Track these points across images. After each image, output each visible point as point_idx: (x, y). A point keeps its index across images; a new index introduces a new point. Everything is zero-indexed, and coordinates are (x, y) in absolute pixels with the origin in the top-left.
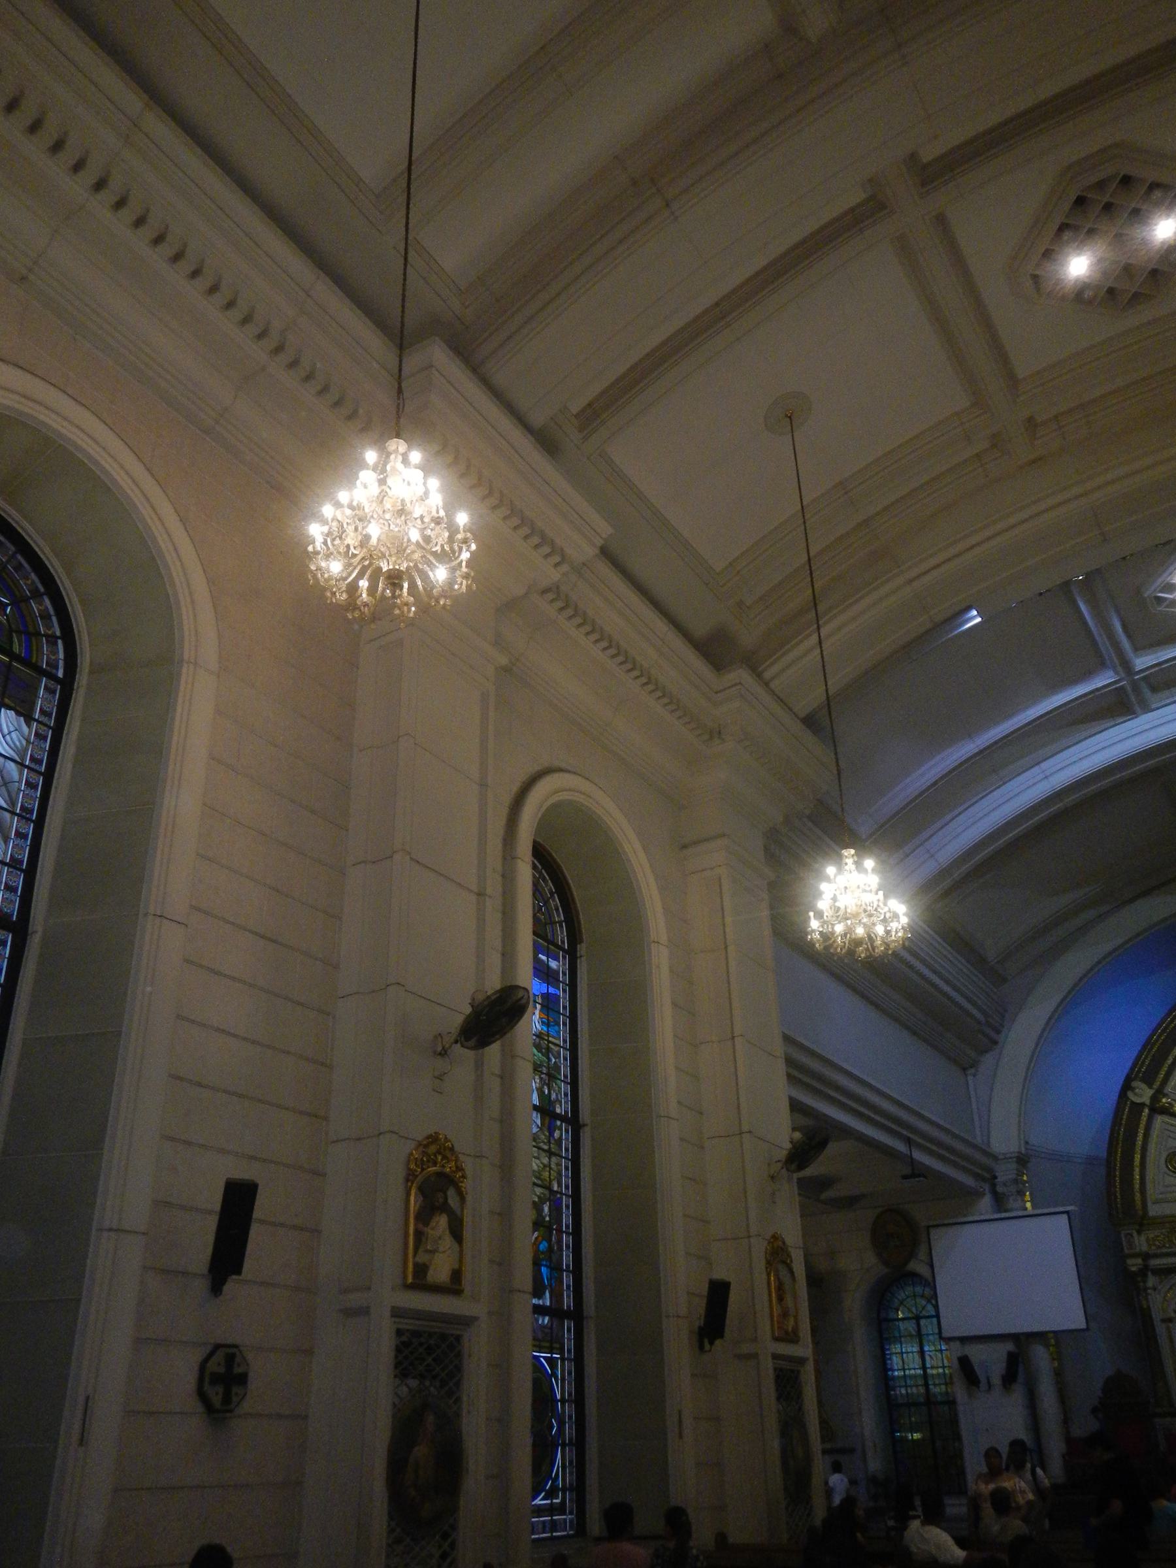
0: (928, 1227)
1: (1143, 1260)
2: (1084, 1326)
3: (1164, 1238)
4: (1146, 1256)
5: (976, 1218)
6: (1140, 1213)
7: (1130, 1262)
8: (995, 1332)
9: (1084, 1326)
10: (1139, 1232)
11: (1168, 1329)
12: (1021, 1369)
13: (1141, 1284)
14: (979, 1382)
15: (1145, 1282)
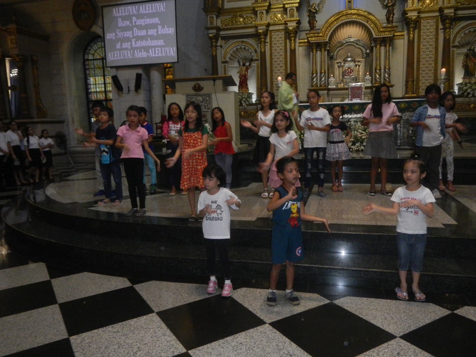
0: (103, 7)
1: (216, 31)
2: (176, 60)
3: (229, 21)
4: (219, 29)
6: (220, 6)
7: (210, 31)
8: (135, 64)
9: (176, 60)
10: (217, 17)
11: (225, 66)
12: (144, 83)
14: (123, 89)
15: (216, 42)
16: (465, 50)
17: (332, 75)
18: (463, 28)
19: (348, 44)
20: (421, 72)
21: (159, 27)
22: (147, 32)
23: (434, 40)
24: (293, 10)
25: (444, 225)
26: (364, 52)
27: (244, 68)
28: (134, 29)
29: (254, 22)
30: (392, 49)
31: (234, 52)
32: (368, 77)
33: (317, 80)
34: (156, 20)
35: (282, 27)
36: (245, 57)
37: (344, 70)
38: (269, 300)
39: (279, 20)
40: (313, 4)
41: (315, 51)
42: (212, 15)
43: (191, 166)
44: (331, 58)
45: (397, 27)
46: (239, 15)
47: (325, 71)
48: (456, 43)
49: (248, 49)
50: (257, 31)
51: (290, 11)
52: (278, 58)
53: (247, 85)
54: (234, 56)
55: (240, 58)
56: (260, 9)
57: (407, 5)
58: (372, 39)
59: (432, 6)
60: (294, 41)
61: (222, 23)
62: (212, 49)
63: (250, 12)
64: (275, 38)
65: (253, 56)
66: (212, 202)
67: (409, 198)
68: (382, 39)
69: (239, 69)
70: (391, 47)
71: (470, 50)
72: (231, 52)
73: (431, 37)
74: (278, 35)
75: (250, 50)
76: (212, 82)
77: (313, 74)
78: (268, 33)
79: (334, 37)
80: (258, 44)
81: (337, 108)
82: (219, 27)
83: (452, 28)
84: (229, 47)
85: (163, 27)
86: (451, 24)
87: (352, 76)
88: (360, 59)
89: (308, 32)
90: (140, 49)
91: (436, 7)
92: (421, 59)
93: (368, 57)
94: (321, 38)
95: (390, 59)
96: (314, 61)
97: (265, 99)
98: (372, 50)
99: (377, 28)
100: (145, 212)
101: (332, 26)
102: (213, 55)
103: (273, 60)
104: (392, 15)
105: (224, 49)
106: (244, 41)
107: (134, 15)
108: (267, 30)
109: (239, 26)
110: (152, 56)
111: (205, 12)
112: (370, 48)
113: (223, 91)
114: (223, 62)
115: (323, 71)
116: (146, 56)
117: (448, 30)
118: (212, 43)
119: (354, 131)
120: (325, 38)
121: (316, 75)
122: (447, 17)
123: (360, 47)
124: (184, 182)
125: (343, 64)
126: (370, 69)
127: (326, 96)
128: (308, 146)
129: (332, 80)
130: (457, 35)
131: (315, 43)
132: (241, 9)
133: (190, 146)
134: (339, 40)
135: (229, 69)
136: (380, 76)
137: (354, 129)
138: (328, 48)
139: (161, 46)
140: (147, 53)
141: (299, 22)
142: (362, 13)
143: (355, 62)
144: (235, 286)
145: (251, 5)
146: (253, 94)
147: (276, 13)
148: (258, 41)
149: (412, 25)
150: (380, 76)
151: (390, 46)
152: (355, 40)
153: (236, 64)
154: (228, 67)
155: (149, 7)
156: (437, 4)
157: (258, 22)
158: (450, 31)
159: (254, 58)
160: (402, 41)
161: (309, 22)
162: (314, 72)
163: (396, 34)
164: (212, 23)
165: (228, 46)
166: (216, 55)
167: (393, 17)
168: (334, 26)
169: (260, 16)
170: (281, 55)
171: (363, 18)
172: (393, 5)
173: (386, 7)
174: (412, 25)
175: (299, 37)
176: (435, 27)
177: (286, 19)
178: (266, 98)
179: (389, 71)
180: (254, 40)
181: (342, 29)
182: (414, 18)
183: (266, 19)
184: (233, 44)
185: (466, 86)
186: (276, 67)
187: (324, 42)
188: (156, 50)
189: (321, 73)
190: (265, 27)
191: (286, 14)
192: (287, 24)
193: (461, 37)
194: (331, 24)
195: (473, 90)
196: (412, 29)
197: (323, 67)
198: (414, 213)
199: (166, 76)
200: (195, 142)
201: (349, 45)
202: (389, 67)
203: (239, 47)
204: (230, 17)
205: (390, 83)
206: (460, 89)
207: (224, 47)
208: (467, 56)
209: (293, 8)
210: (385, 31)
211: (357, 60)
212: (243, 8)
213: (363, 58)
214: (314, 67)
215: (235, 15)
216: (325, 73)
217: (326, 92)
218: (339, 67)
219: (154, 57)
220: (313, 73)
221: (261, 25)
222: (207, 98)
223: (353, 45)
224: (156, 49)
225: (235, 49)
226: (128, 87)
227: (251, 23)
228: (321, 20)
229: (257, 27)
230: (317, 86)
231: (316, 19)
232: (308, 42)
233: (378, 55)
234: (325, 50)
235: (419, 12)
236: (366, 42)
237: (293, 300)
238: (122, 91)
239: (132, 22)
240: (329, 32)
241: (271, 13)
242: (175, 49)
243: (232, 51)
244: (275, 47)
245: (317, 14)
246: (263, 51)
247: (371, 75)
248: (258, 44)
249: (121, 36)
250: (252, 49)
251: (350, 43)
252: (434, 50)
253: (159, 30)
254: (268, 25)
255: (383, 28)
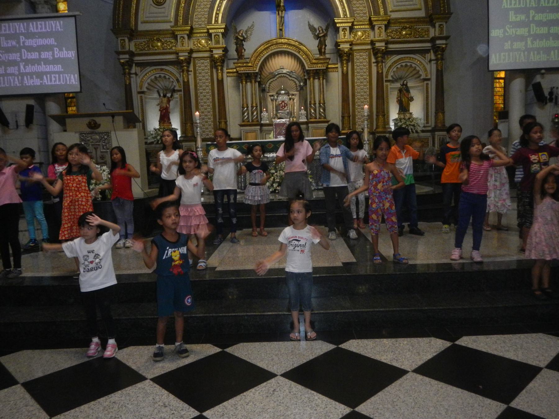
1: (129, 56)
3: (145, 45)
4: (132, 54)
5: (14, 17)
10: (130, 40)
11: (141, 97)
12: (37, 116)
13: (127, 70)
15: (130, 69)
16: (398, 85)
17: (265, 109)
18: (395, 62)
19: (280, 75)
20: (356, 107)
21: (55, 49)
22: (40, 55)
23: (368, 73)
24: (218, 35)
25: (343, 263)
26: (298, 85)
27: (165, 100)
28: (23, 50)
29: (174, 48)
30: (327, 81)
31: (151, 80)
32: (303, 112)
33: (248, 114)
34: (51, 41)
35: (207, 54)
36: (165, 87)
37: (277, 103)
38: (156, 355)
39: (203, 47)
40: (240, 31)
41: (244, 83)
42: (123, 37)
43: (73, 213)
44: (263, 90)
45: (329, 59)
46: (157, 39)
47: (256, 104)
48: (390, 78)
49: (169, 78)
50: (178, 57)
51: (215, 37)
52: (204, 90)
53: (169, 119)
54: (152, 86)
55: (160, 88)
56: (181, 33)
57: (339, 37)
58: (304, 70)
59: (363, 39)
60: (221, 70)
61: (136, 48)
62: (125, 77)
63: (169, 36)
64: (200, 67)
65: (175, 86)
66: (89, 252)
67: (296, 237)
68: (315, 71)
69: (159, 101)
70: (325, 80)
71: (403, 85)
72: (149, 81)
73: (365, 70)
74: (203, 63)
75: (171, 80)
76: (110, 118)
77: (243, 108)
78: (191, 60)
79: (266, 67)
80: (180, 72)
81: (258, 148)
82: (132, 52)
83: (385, 62)
84: (146, 74)
85: (61, 50)
86: (383, 58)
87: (286, 110)
88: (294, 92)
89: (236, 61)
90: (31, 75)
91: (367, 39)
92: (356, 93)
93: (302, 91)
94: (251, 69)
95: (325, 92)
96: (244, 93)
97: (166, 137)
98: (305, 83)
99: (309, 60)
100: (21, 272)
101: (262, 55)
102: (126, 85)
103: (199, 92)
104: (324, 47)
105: (139, 77)
106: (163, 69)
107: (22, 34)
108: (190, 57)
109: (157, 51)
110: (47, 84)
111: (114, 33)
112: (304, 81)
113: (125, 128)
114: (139, 93)
115: (254, 105)
116: (39, 84)
117: (380, 64)
118: (124, 69)
119: (280, 171)
120: (255, 69)
121: (247, 109)
122: (379, 50)
123: (293, 79)
124: (63, 232)
125: (276, 97)
126: (304, 102)
127: (259, 132)
128: (225, 187)
129: (265, 115)
130: (390, 69)
131: (244, 73)
132: (159, 32)
133: (72, 190)
134: (272, 71)
135: (147, 100)
136: (315, 110)
137: (279, 169)
138: (259, 80)
139: (59, 73)
140: (40, 81)
141: (226, 50)
142: (293, 43)
143: (289, 96)
144: (121, 345)
145: (169, 28)
146: (177, 129)
147: (199, 38)
148: (180, 69)
149: (345, 58)
150: (315, 110)
151: (323, 79)
152: (288, 72)
153: (156, 95)
154: (146, 98)
155: (41, 25)
156: (369, 37)
157: (179, 47)
158: (382, 65)
159: (176, 89)
160: (337, 73)
161: (237, 50)
162: (245, 105)
163: (330, 66)
164: (123, 47)
165: (143, 75)
166: (130, 84)
167: (325, 49)
168: (264, 55)
169: (181, 40)
170: (207, 86)
171: (294, 49)
172: (325, 36)
173: (317, 37)
174: (345, 58)
175: (228, 66)
176: (367, 60)
177: (211, 46)
178: (168, 136)
179: (325, 106)
180: (175, 67)
181: (273, 60)
182: (346, 50)
183: (189, 45)
184: (150, 71)
185: (401, 122)
186: (202, 100)
187: (254, 73)
188: (53, 77)
189: (252, 107)
190: (187, 54)
191: (212, 41)
192: (212, 51)
193: (394, 71)
194: (261, 53)
195: (407, 125)
196: (345, 62)
197: (254, 101)
198: (300, 251)
199: (68, 108)
200: (78, 186)
201: (281, 77)
202: (324, 101)
203: (158, 75)
204: (146, 40)
205: (325, 118)
206: (396, 125)
207: (140, 74)
208: (400, 91)
209: (218, 34)
210: (317, 63)
211: (291, 93)
212: (160, 30)
213: (297, 91)
214: (245, 100)
215: (151, 39)
216: (257, 107)
217: (259, 127)
218: (272, 100)
219: (48, 85)
220: (243, 107)
221: (183, 51)
222: (106, 137)
223: (286, 76)
224: (53, 75)
225: (153, 77)
226: (17, 122)
227: (171, 48)
228: (250, 48)
229: (177, 54)
230: (249, 121)
231: (245, 47)
232: (237, 72)
233: (312, 88)
234: (256, 82)
235: (352, 44)
236: (299, 74)
237: (182, 353)
238: (8, 127)
239: (20, 42)
240: (259, 62)
241: (194, 38)
242: (77, 76)
243: (150, 79)
244: (200, 77)
245: (244, 41)
246: (186, 80)
247: (306, 109)
248: (180, 72)
249: (5, 58)
250: (173, 78)
251: (282, 75)
252: (368, 84)
253: (56, 52)
254: (191, 52)
255: (315, 59)
